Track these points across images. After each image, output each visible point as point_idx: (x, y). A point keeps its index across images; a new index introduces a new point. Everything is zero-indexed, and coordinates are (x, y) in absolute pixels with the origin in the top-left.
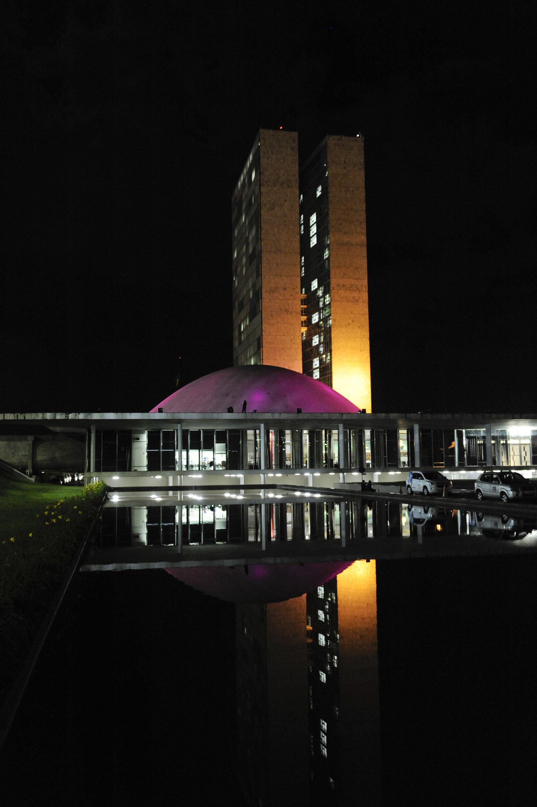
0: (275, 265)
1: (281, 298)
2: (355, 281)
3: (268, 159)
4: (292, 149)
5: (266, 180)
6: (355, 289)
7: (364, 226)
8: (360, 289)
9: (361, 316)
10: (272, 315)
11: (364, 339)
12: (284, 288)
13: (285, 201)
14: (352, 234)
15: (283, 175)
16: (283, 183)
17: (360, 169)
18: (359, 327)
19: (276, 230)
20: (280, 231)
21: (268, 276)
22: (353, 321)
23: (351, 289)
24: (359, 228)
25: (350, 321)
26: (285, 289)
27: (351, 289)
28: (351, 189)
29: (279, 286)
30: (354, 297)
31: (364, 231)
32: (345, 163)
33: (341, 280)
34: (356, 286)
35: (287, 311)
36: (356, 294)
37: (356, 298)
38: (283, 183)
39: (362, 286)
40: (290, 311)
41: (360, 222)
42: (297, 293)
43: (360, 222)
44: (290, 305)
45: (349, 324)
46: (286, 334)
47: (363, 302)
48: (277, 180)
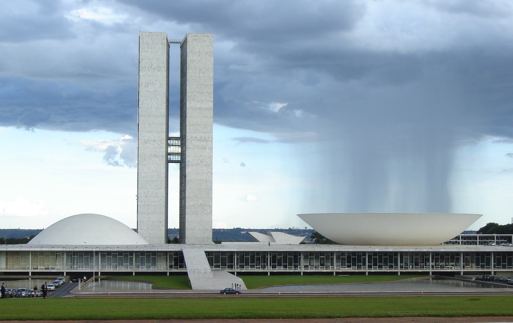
7: (212, 96)
13: (156, 81)
14: (203, 101)
16: (155, 68)
17: (210, 56)
19: (149, 101)
21: (143, 133)
22: (201, 162)
24: (208, 98)
30: (202, 146)
31: (212, 99)
35: (155, 156)
36: (204, 143)
38: (155, 68)
45: (199, 164)
47: (209, 148)
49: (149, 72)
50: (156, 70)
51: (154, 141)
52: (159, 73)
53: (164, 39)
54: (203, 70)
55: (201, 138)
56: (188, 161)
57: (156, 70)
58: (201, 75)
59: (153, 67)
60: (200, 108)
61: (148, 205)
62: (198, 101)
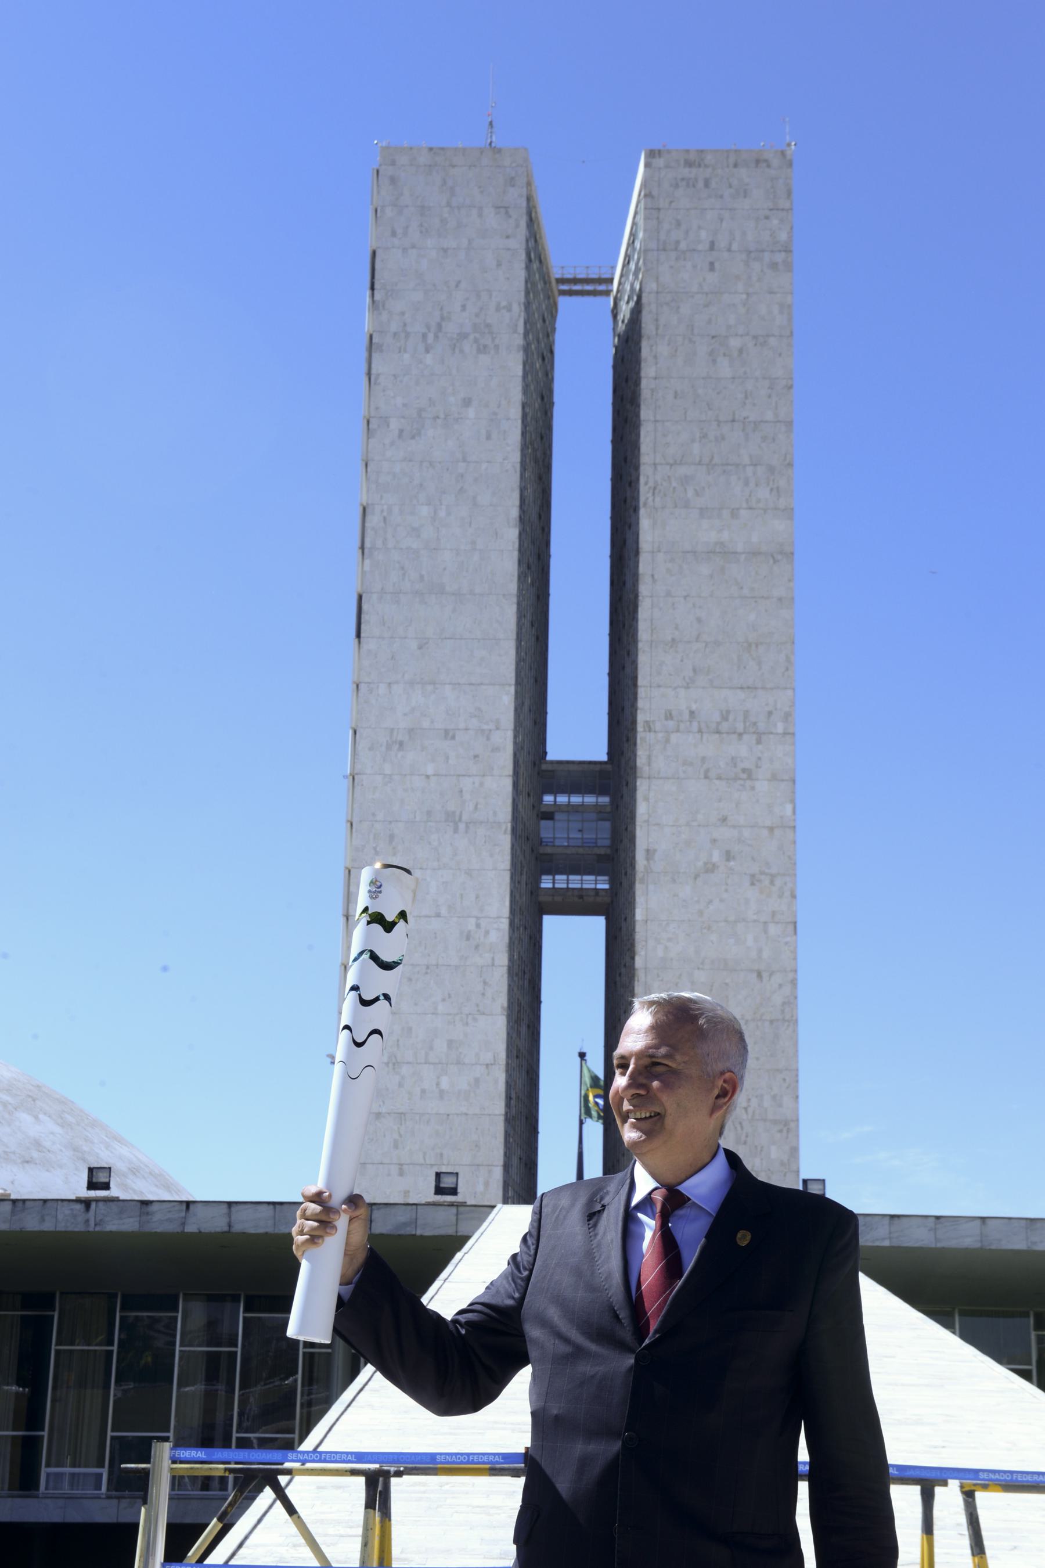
0: (414, 645)
1: (430, 772)
2: (742, 695)
3: (405, 250)
4: (503, 209)
5: (394, 327)
6: (740, 727)
8: (762, 726)
9: (765, 832)
10: (392, 837)
11: (773, 929)
12: (446, 731)
13: (467, 402)
14: (734, 514)
15: (464, 308)
17: (774, 266)
18: (754, 880)
19: (425, 511)
20: (442, 514)
21: (382, 689)
22: (728, 856)
23: (725, 726)
24: (763, 493)
25: (716, 857)
26: (448, 734)
27: (725, 726)
28: (735, 343)
29: (426, 724)
30: (734, 761)
32: (712, 246)
33: (682, 692)
34: (746, 714)
35: (453, 819)
36: (743, 749)
37: (747, 765)
38: (463, 336)
39: (770, 713)
40: (465, 818)
41: (771, 469)
42: (496, 749)
43: (771, 469)
44: (467, 796)
45: (710, 868)
46: (444, 911)
47: (774, 778)
48: (439, 326)
49: (429, 359)
50: (468, 346)
51: (448, 734)
52: (484, 359)
53: (511, 181)
54: (735, 343)
55: (725, 718)
56: (649, 853)
57: (468, 346)
58: (725, 368)
59: (451, 328)
60: (724, 553)
61: (401, 1116)
62: (703, 512)
